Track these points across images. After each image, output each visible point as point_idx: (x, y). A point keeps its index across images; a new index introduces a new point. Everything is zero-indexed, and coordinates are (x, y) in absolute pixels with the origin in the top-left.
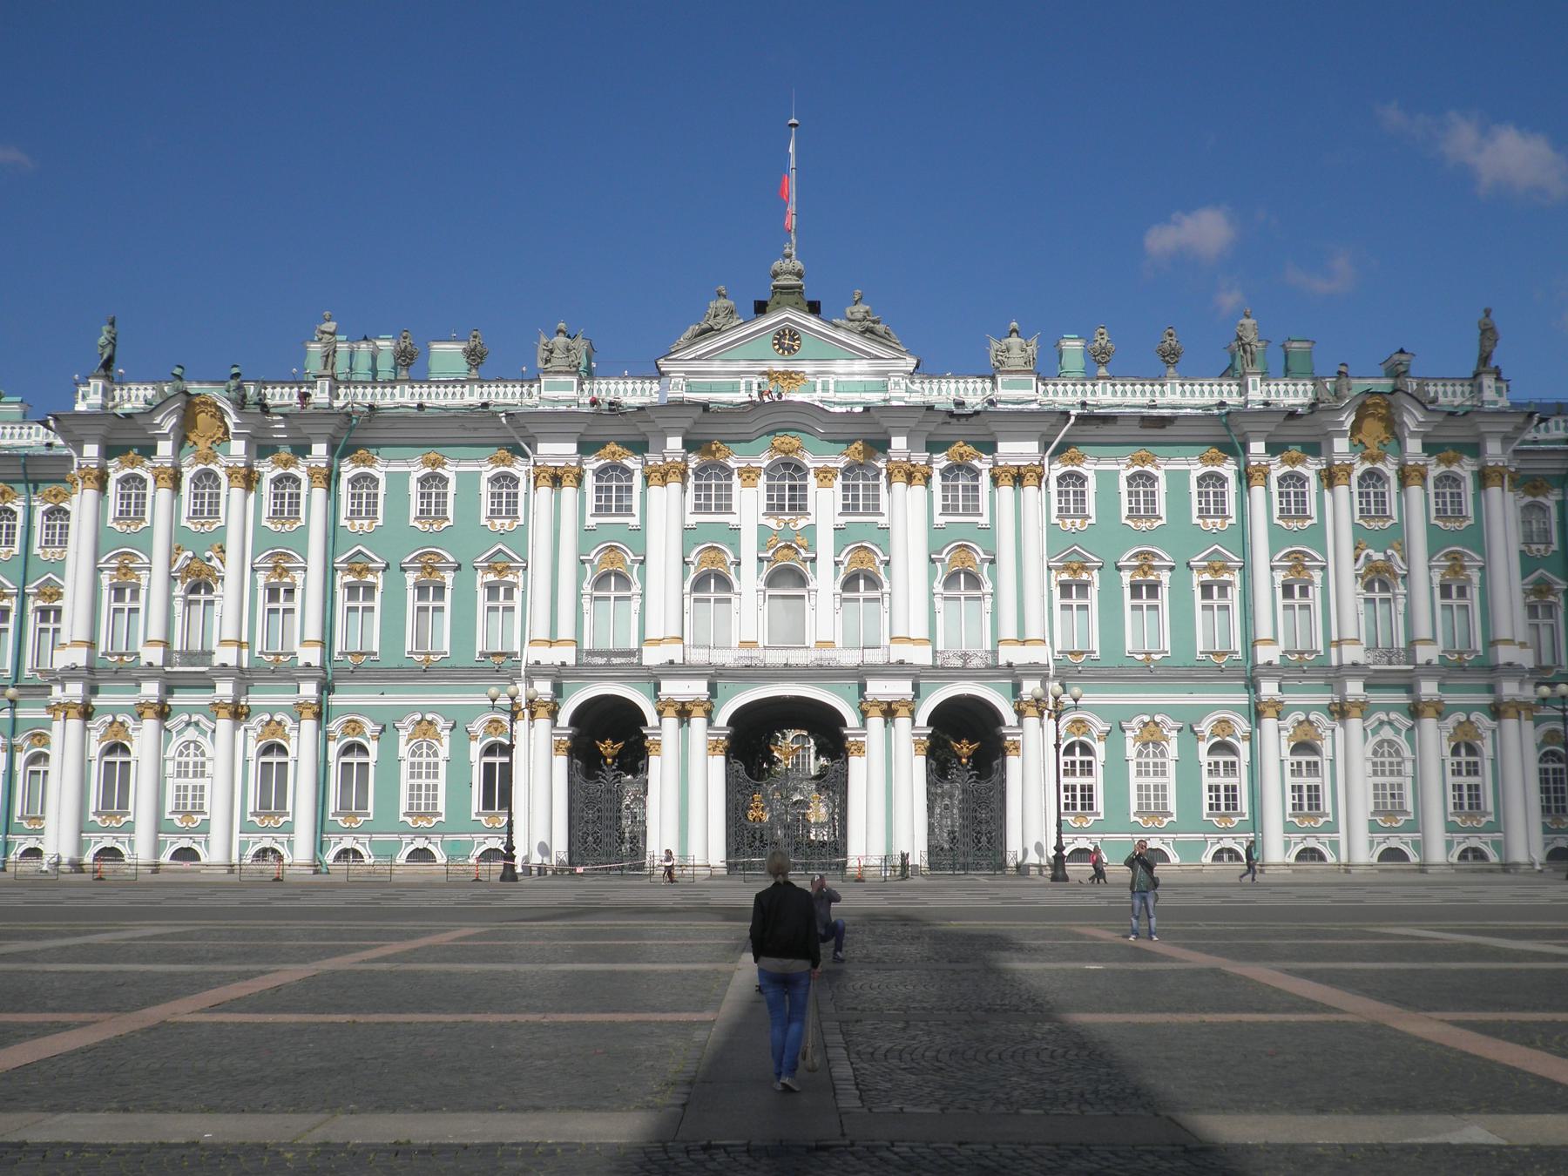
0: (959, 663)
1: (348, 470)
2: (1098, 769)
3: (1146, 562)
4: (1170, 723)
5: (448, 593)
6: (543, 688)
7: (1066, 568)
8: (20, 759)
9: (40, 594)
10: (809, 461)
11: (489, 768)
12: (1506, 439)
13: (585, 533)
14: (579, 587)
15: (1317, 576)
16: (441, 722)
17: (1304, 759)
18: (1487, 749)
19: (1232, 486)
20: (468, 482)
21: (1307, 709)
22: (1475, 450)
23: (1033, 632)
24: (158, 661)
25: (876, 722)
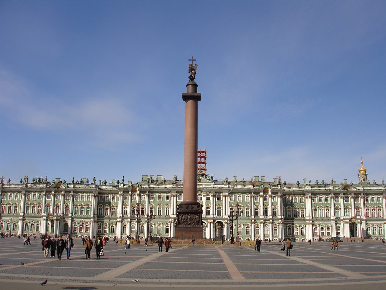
5: (162, 209)
7: (231, 207)
9: (112, 207)
10: (202, 194)
11: (166, 229)
12: (281, 192)
15: (259, 208)
17: (257, 229)
18: (277, 228)
19: (250, 197)
23: (227, 214)
25: (209, 224)
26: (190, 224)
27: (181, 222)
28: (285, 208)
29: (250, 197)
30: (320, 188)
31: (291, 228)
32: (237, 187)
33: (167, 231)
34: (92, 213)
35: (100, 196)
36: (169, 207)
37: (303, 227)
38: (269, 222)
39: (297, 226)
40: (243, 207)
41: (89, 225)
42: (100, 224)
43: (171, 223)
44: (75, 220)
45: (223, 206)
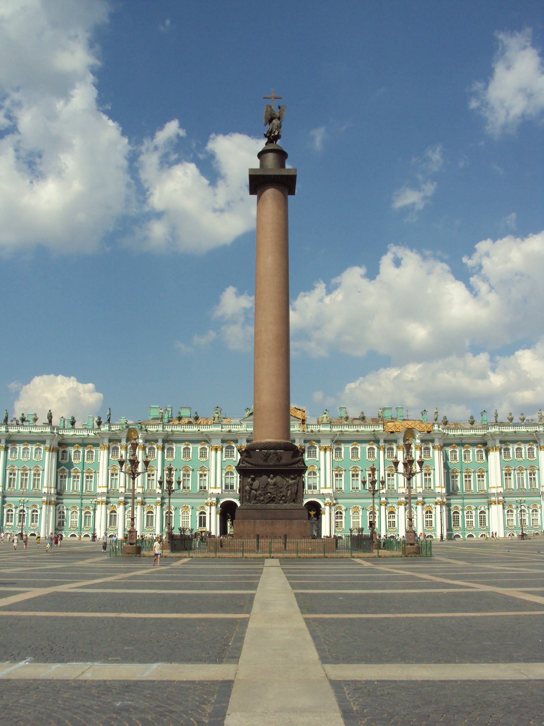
0: (311, 493)
1: (167, 446)
2: (343, 518)
3: (355, 469)
4: (360, 507)
6: (214, 500)
7: (337, 471)
8: (83, 513)
9: (87, 472)
11: (200, 517)
13: (222, 462)
14: (222, 475)
16: (190, 507)
17: (392, 515)
20: (195, 449)
21: (392, 503)
22: (433, 441)
23: (328, 485)
24: (124, 492)
26: (272, 500)
27: (249, 496)
28: (446, 471)
29: (376, 451)
30: (517, 429)
31: (458, 513)
32: (350, 430)
33: (202, 522)
34: (45, 485)
35: (61, 450)
36: (205, 472)
37: (483, 509)
38: (416, 501)
39: (471, 509)
40: (362, 471)
41: (39, 511)
42: (61, 509)
43: (211, 505)
44: (7, 499)
45: (320, 469)
